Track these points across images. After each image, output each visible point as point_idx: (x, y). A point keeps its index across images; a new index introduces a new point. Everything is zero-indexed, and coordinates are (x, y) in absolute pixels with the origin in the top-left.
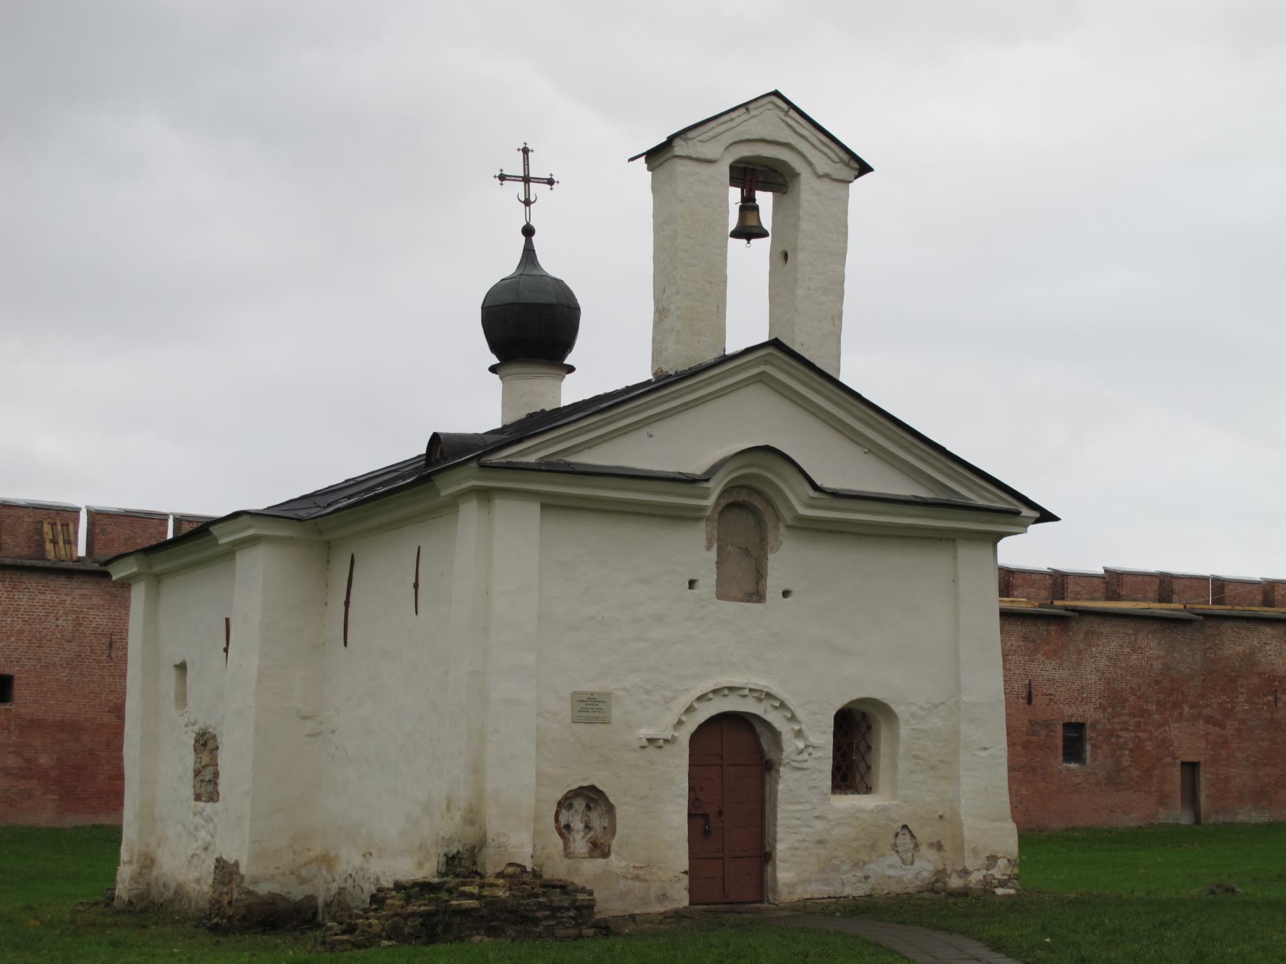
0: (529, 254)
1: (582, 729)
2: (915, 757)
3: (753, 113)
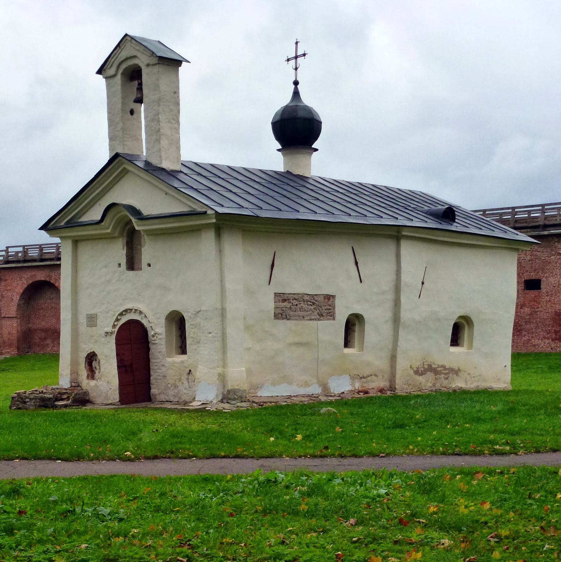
0: (296, 94)
1: (89, 329)
2: (192, 337)
3: (122, 47)
